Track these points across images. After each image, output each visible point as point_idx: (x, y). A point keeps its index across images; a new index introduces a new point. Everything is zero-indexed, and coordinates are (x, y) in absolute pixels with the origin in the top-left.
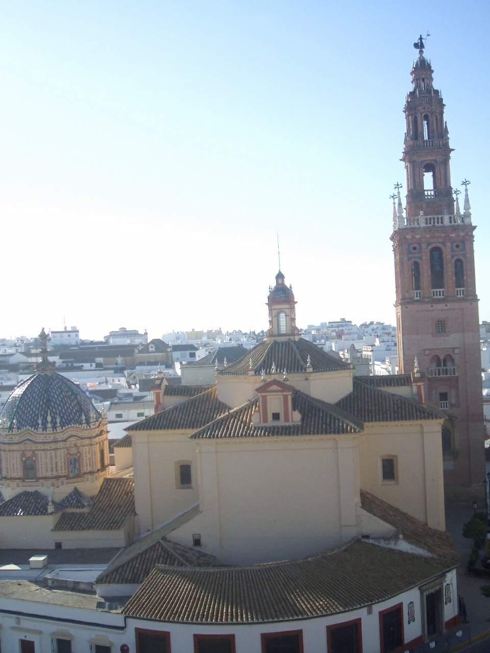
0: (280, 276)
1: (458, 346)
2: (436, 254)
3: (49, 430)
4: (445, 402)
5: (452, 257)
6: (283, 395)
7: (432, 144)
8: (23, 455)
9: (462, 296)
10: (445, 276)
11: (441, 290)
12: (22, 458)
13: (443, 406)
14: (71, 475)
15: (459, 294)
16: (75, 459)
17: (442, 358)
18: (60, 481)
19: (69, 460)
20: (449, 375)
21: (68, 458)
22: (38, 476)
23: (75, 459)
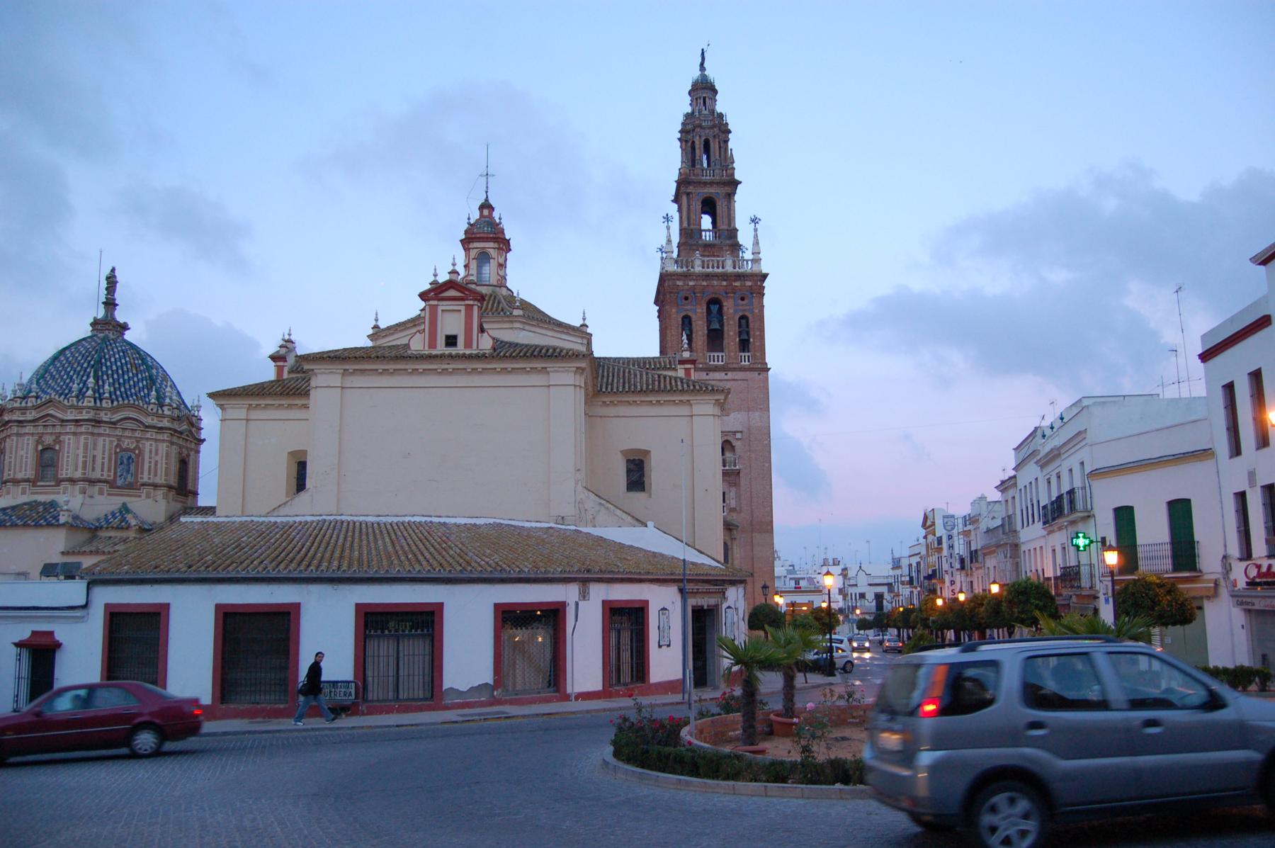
0: (486, 206)
2: (715, 308)
3: (88, 402)
5: (736, 311)
6: (466, 305)
9: (747, 363)
10: (726, 336)
11: (720, 354)
12: (37, 446)
14: (119, 482)
15: (743, 360)
16: (129, 457)
18: (97, 488)
19: (119, 457)
21: (116, 453)
22: (59, 476)
23: (129, 457)
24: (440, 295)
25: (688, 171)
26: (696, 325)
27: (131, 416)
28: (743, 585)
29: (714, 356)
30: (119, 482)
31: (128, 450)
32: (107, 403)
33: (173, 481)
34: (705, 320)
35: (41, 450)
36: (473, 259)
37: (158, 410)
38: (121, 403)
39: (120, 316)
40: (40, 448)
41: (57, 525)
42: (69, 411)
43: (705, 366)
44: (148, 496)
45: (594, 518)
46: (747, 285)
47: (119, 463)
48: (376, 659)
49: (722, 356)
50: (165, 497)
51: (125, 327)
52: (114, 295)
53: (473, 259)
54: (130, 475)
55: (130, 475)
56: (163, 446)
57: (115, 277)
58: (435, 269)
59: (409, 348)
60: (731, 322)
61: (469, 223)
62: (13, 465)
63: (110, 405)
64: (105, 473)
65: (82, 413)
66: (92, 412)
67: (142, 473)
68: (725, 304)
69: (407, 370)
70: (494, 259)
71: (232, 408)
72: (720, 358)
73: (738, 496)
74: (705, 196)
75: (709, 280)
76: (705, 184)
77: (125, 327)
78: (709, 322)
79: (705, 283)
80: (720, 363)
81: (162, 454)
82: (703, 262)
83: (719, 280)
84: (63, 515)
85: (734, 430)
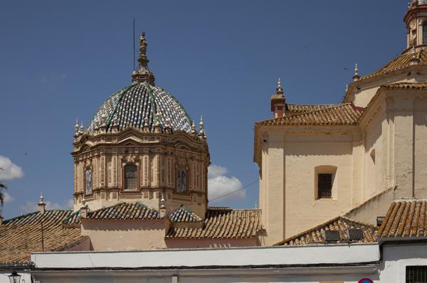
40: (124, 164)
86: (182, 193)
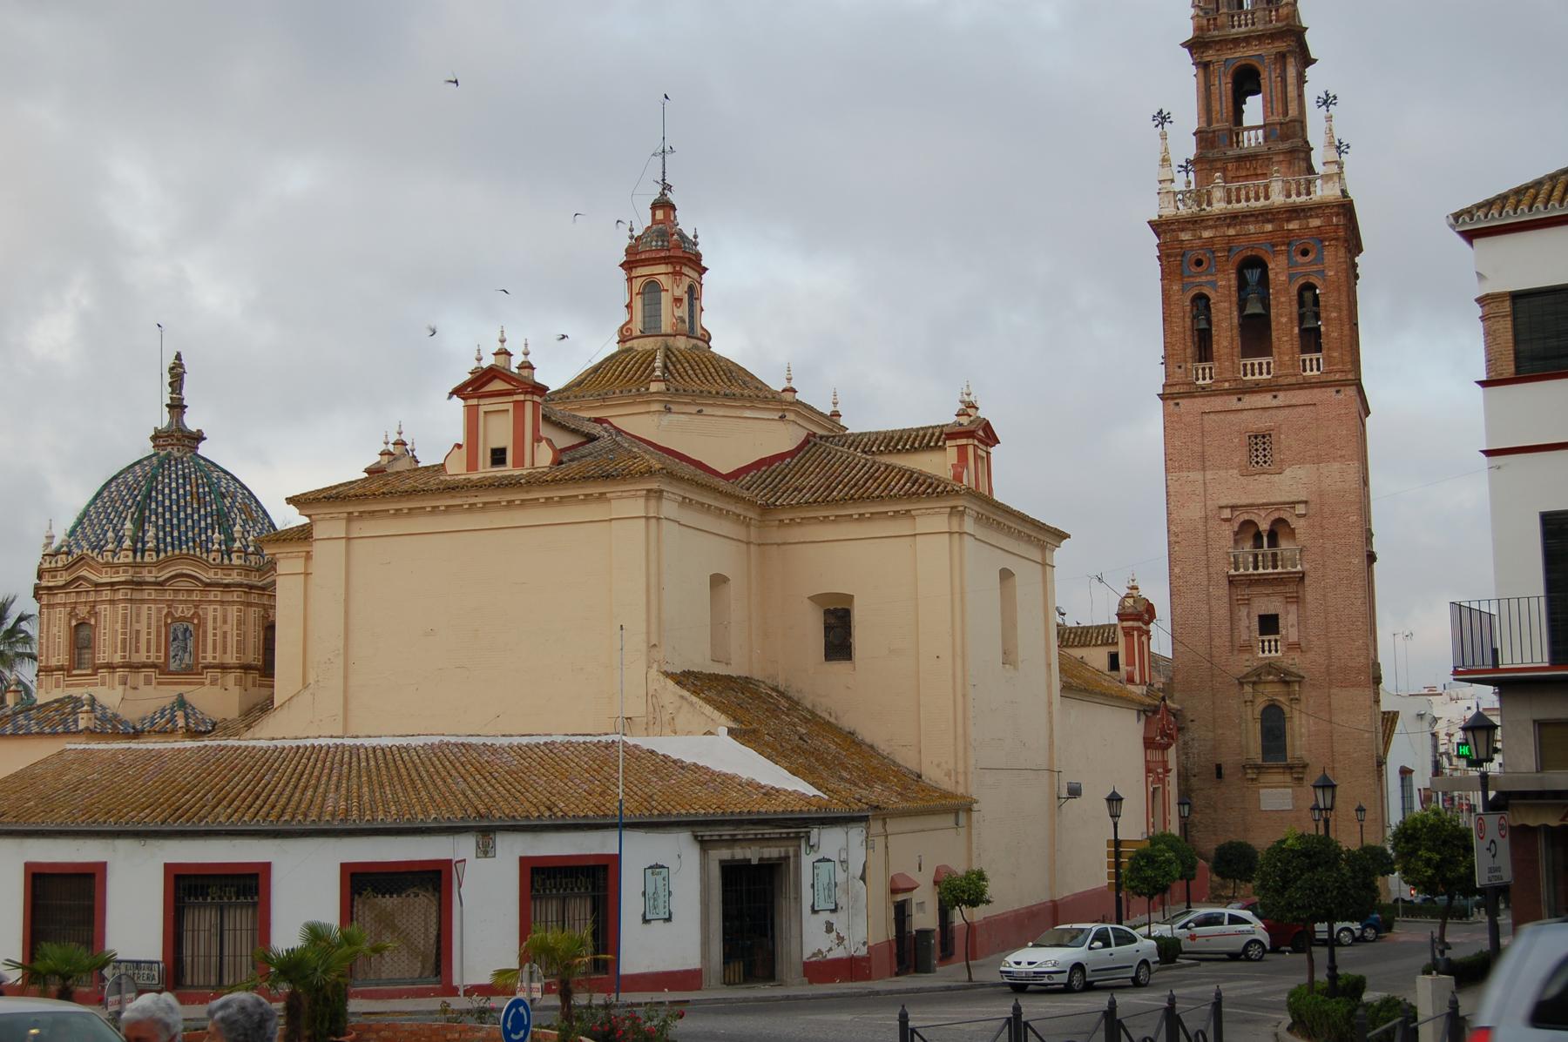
0: (663, 205)
1: (1304, 499)
2: (1253, 275)
4: (1272, 637)
5: (1291, 277)
7: (1253, 19)
8: (72, 615)
9: (1315, 372)
10: (1273, 325)
11: (1264, 360)
13: (1267, 648)
14: (173, 666)
15: (1308, 367)
16: (186, 630)
17: (1264, 526)
20: (1279, 570)
21: (166, 624)
22: (97, 662)
23: (186, 630)
24: (483, 390)
25: (1205, 22)
26: (1218, 310)
27: (184, 571)
28: (863, 824)
29: (1253, 365)
30: (173, 666)
31: (182, 619)
32: (150, 555)
33: (253, 657)
34: (1234, 299)
35: (75, 626)
36: (637, 294)
37: (222, 559)
38: (185, 551)
39: (191, 422)
40: (74, 623)
41: (74, 733)
42: (104, 570)
43: (1234, 385)
44: (214, 682)
45: (673, 719)
46: (1311, 225)
47: (172, 639)
48: (238, 933)
49: (1268, 364)
50: (239, 682)
51: (199, 437)
52: (180, 393)
53: (637, 294)
54: (187, 655)
55: (187, 655)
56: (232, 610)
57: (181, 366)
58: (479, 350)
59: (445, 470)
60: (1283, 299)
61: (631, 237)
62: (44, 647)
63: (155, 560)
64: (153, 654)
65: (119, 573)
66: (131, 571)
67: (205, 651)
68: (1270, 266)
69: (424, 508)
70: (667, 290)
71: (287, 558)
72: (1265, 366)
73: (1302, 621)
74: (1237, 64)
75: (1241, 223)
76: (1236, 42)
77: (199, 437)
78: (1242, 305)
79: (1232, 232)
80: (1265, 376)
81: (233, 625)
82: (1229, 191)
83: (1258, 222)
84: (83, 718)
85: (1294, 499)
86: (185, 669)
